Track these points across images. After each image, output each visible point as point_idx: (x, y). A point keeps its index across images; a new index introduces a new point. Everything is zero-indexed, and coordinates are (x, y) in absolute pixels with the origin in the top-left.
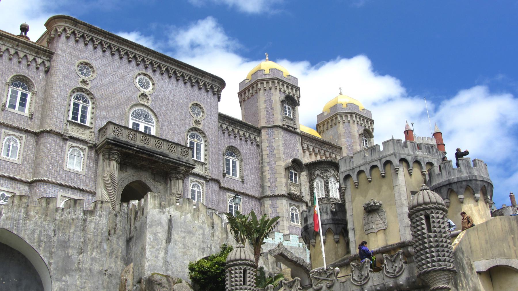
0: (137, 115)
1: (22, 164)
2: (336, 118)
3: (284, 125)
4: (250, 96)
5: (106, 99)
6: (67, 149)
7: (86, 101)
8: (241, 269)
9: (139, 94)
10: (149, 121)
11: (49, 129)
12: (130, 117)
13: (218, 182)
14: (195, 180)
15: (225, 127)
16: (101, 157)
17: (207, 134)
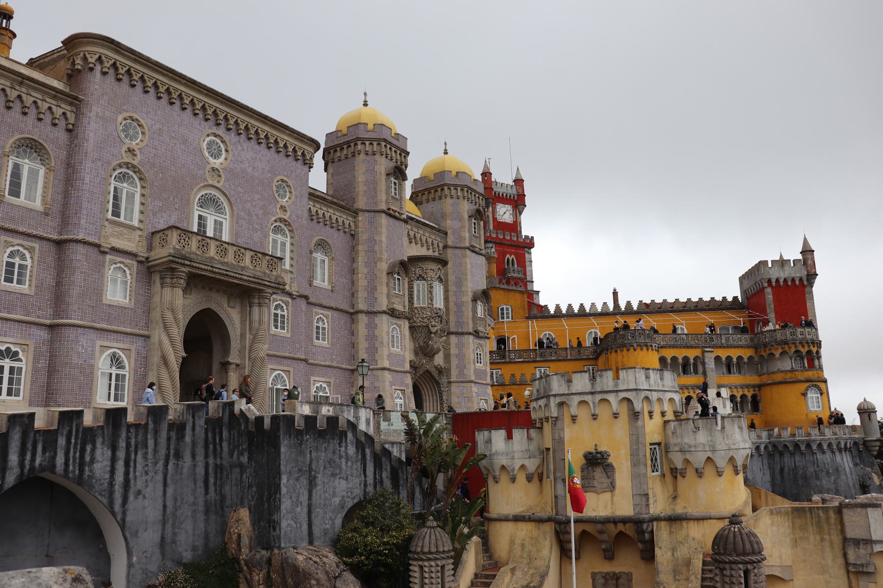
0: (206, 202)
1: (36, 294)
2: (442, 189)
3: (389, 209)
4: (343, 157)
5: (162, 179)
6: (107, 268)
7: (132, 183)
8: (438, 566)
9: (208, 168)
10: (219, 209)
11: (80, 237)
12: (196, 207)
13: (306, 298)
14: (279, 298)
15: (314, 210)
16: (157, 278)
17: (294, 226)
